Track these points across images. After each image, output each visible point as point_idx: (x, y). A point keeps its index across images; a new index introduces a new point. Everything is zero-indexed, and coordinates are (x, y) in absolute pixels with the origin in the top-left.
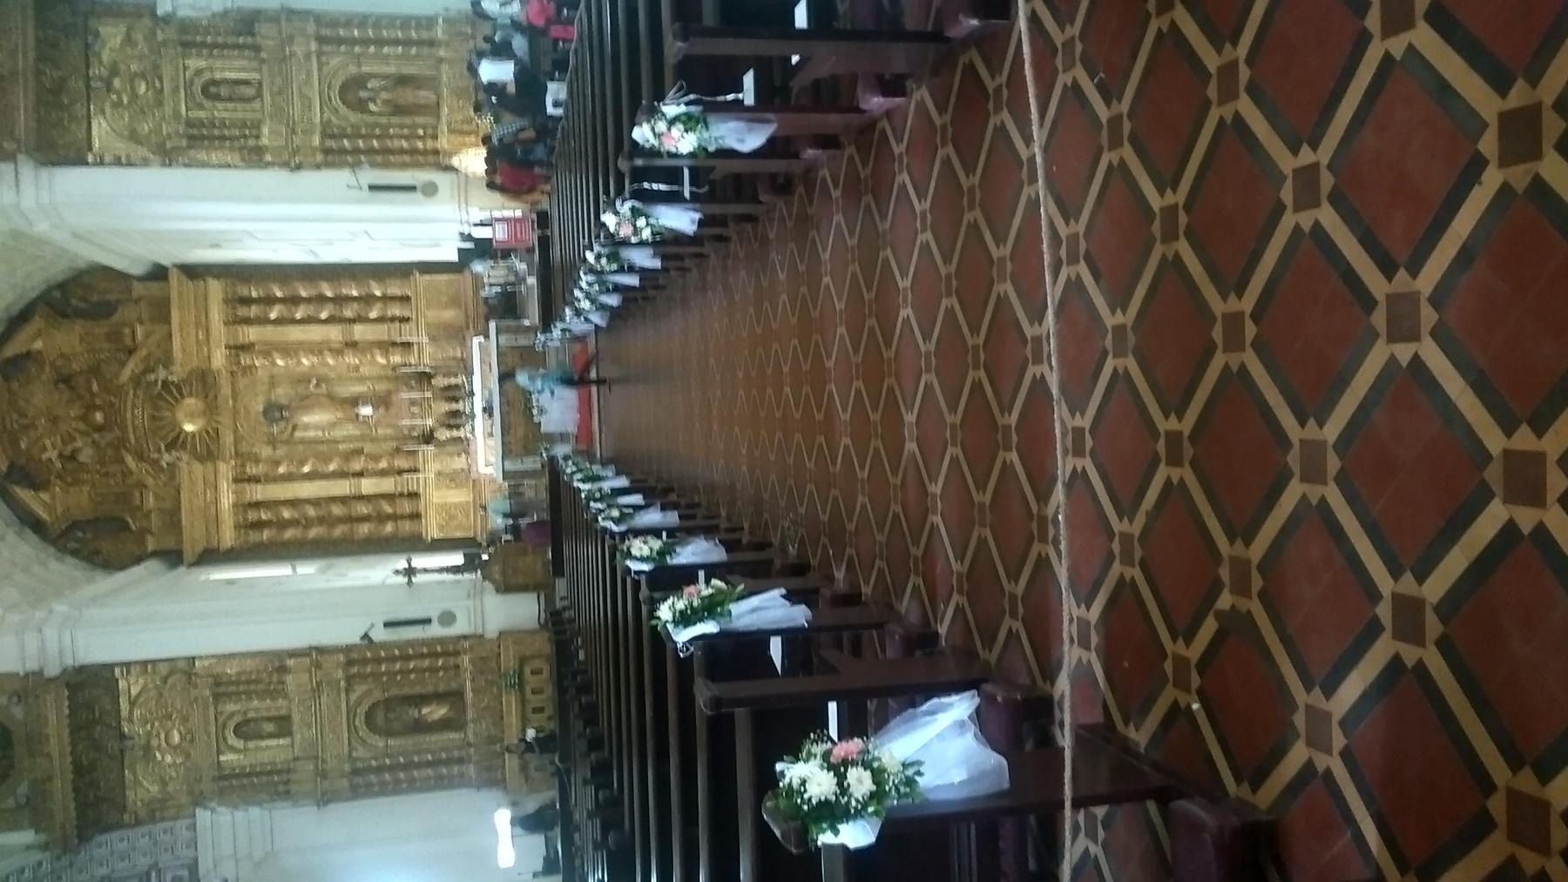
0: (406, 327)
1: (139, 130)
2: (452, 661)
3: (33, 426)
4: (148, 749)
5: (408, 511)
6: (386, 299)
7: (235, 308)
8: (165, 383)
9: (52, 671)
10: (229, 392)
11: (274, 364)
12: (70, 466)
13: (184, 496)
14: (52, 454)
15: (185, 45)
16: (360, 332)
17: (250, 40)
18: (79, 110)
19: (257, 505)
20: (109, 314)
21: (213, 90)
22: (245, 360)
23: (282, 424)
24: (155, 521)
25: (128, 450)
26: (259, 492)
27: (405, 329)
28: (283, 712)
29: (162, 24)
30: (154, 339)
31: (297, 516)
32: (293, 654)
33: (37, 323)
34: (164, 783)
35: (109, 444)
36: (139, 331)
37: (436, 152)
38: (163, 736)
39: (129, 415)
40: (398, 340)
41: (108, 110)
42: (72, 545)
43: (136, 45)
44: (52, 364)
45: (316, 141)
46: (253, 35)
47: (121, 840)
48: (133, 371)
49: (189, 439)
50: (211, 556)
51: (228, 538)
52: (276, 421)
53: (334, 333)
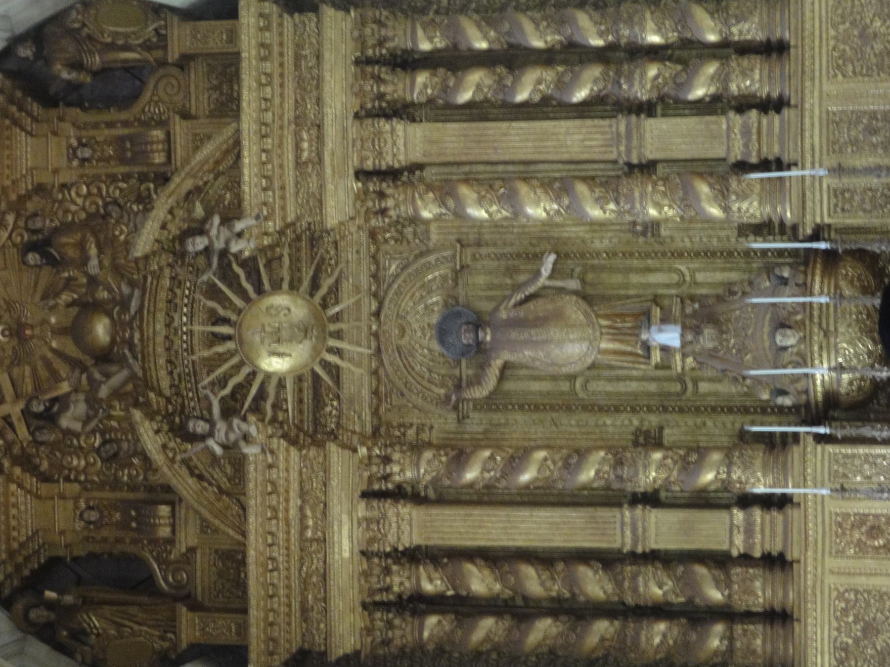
8: (224, 253)
11: (459, 214)
13: (253, 522)
27: (770, 125)
30: (208, 150)
31: (498, 587)
35: (117, 394)
36: (180, 129)
48: (164, 227)
49: (271, 390)
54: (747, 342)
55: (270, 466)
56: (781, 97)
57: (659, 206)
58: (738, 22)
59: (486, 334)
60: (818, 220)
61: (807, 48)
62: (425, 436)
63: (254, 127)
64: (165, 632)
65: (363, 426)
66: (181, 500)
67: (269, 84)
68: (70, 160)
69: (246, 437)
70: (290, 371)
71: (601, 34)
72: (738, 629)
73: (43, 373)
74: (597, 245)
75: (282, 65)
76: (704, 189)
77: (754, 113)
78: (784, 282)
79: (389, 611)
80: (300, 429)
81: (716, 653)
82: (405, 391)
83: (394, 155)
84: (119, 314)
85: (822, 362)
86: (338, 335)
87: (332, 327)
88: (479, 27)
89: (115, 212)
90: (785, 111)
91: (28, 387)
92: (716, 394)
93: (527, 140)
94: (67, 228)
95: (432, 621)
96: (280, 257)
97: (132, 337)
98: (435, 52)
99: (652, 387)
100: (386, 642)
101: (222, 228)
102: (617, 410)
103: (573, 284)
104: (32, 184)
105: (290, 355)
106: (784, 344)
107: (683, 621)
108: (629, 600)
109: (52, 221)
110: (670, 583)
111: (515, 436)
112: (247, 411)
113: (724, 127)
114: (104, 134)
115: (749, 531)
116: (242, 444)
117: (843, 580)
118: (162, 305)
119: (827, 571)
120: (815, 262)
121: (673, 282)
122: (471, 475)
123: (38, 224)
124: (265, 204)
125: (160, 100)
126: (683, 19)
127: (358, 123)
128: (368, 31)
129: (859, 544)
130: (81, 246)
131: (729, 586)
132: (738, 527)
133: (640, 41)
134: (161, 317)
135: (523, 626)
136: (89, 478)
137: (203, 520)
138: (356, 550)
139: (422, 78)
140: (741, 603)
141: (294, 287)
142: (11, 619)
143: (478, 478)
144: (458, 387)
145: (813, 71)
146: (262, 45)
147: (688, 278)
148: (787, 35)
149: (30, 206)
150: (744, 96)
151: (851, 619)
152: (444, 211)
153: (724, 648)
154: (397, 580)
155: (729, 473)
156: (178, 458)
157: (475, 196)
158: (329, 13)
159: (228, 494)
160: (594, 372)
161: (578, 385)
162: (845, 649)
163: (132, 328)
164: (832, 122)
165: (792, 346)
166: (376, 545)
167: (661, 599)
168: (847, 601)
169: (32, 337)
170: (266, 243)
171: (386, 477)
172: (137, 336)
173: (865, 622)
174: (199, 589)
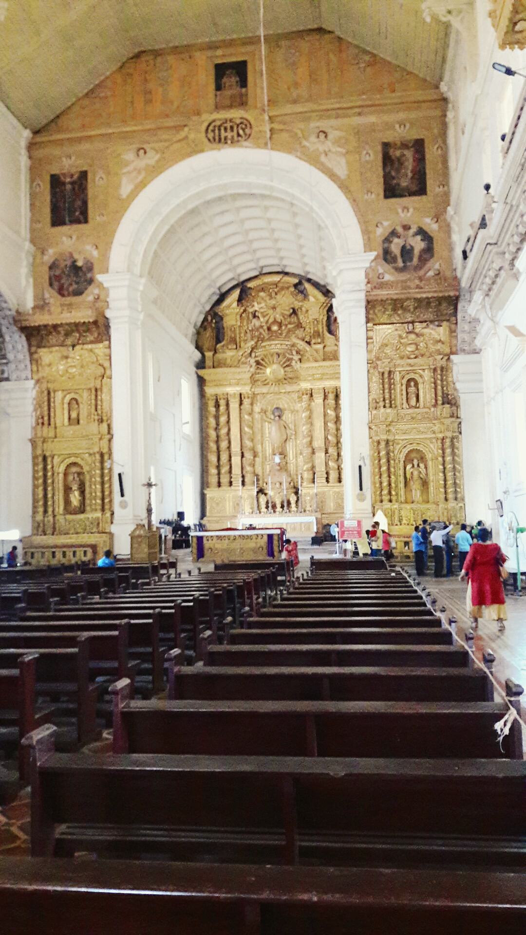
0: (325, 481)
1: (387, 348)
2: (99, 507)
3: (271, 297)
4: (67, 357)
5: (222, 480)
7: (333, 392)
8: (292, 359)
9: (108, 314)
10: (288, 390)
11: (303, 412)
13: (233, 370)
15: (435, 370)
16: (320, 456)
17: (440, 402)
18: (396, 319)
19: (227, 405)
20: (330, 332)
21: (412, 384)
22: (306, 397)
24: (219, 356)
25: (256, 343)
26: (234, 405)
28: (81, 422)
29: (446, 358)
32: (109, 426)
33: (322, 298)
34: (50, 365)
35: (261, 334)
36: (320, 346)
37: (382, 501)
38: (73, 364)
39: (277, 342)
41: (396, 333)
42: (209, 318)
43: (434, 345)
44: (302, 306)
45: (385, 437)
46: (443, 404)
47: (23, 346)
50: (201, 381)
51: (210, 391)
52: (273, 413)
53: (319, 443)
72: (217, 476)
73: (265, 314)
74: (298, 442)
76: (310, 465)
91: (262, 310)
94: (298, 319)
99: (268, 455)
108: (221, 453)
114: (320, 327)
140: (221, 476)
149: (304, 309)
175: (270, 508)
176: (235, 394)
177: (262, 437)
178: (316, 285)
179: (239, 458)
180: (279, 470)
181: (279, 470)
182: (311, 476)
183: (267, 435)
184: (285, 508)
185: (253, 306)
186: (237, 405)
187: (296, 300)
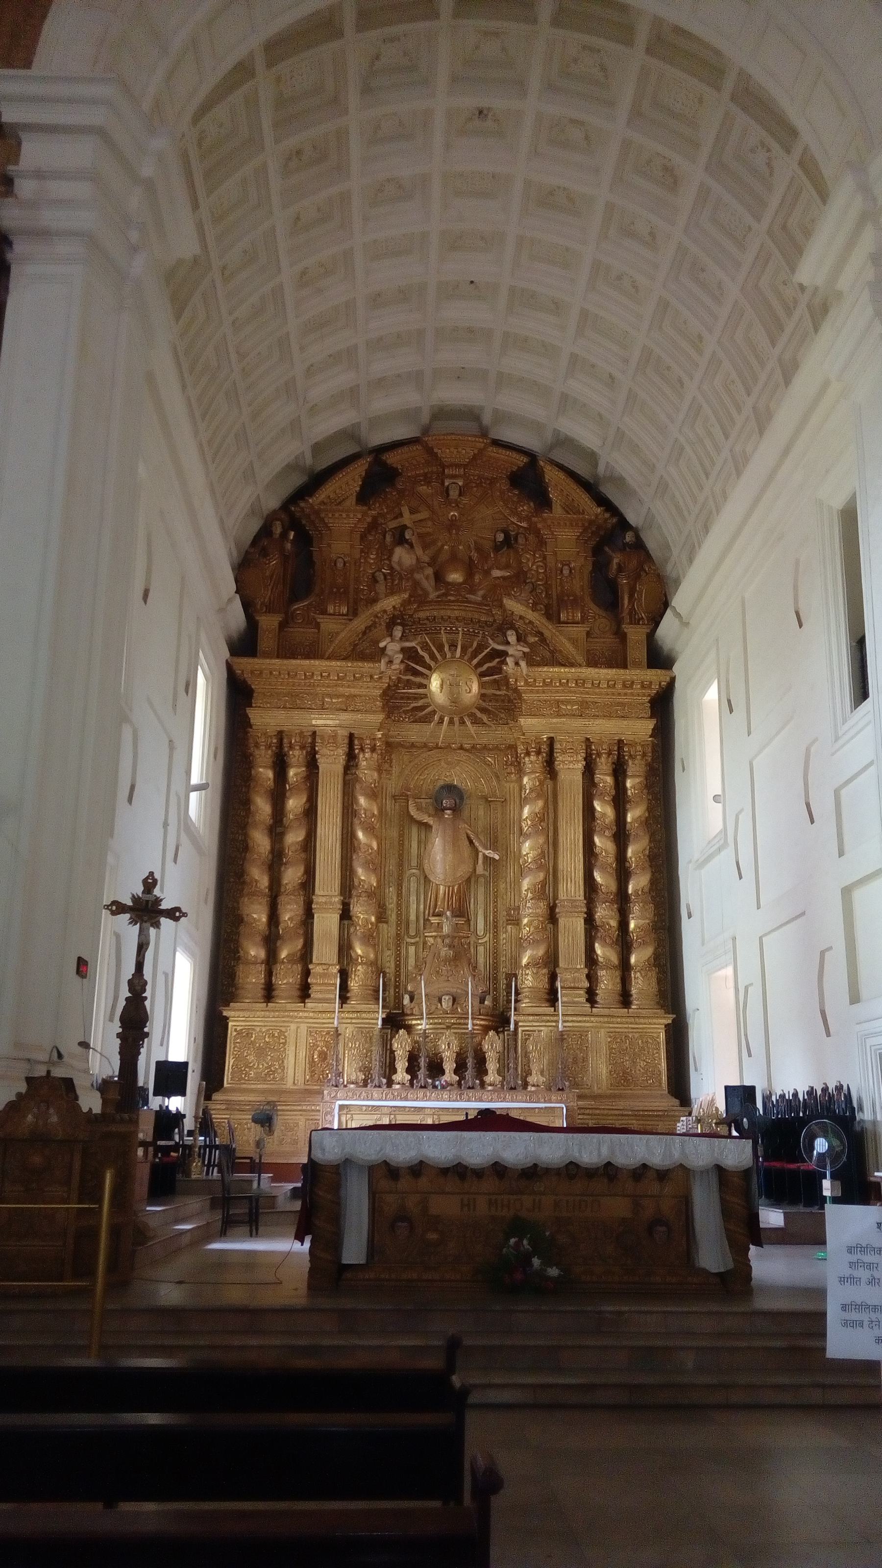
6: (625, 967)
8: (505, 654)
12: (388, 538)
14: (407, 518)
19: (312, 765)
22: (533, 763)
23: (431, 810)
35: (416, 584)
40: (559, 985)
42: (278, 529)
48: (521, 617)
49: (418, 680)
54: (442, 977)
55: (371, 677)
56: (596, 1002)
57: (529, 924)
58: (643, 978)
59: (449, 815)
60: (520, 1024)
61: (628, 1020)
62: (384, 775)
63: (583, 676)
64: (266, 606)
65: (392, 737)
66: (350, 620)
67: (609, 687)
68: (561, 562)
69: (391, 662)
70: (430, 690)
71: (636, 892)
74: (502, 886)
75: (619, 694)
76: (540, 951)
77: (587, 985)
78: (482, 1001)
79: (277, 747)
80: (391, 698)
81: (248, 953)
82: (412, 764)
83: (563, 762)
84: (463, 588)
85: (431, 1024)
86: (451, 722)
87: (456, 719)
88: (640, 817)
89: (528, 588)
90: (589, 1005)
92: (407, 957)
93: (571, 844)
95: (270, 774)
96: (499, 689)
97: (451, 595)
98: (625, 789)
99: (413, 917)
100: (257, 745)
101: (522, 653)
102: (399, 895)
103: (480, 869)
104: (547, 538)
105: (441, 692)
106: (443, 1000)
107: (267, 933)
108: (282, 899)
109: (522, 549)
110: (292, 925)
111: (384, 831)
112: (407, 663)
113: (579, 967)
115: (324, 975)
116: (387, 659)
117: (293, 1035)
118: (470, 615)
119: (298, 1025)
120: (493, 1021)
121: (478, 933)
122: (362, 800)
123: (521, 540)
124: (535, 681)
125: (596, 620)
126: (644, 943)
127: (583, 739)
128: (639, 748)
129: (315, 1046)
130: (507, 567)
131: (289, 962)
132: (327, 969)
133: (631, 916)
134: (463, 614)
135: (266, 831)
136: (362, 565)
137: (338, 633)
138: (316, 729)
139: (609, 780)
141: (483, 696)
142: (274, 512)
143: (361, 806)
144: (416, 797)
145: (612, 1023)
146: (633, 683)
147: (480, 941)
148: (635, 1007)
150: (597, 979)
151: (267, 1040)
152: (527, 791)
153: (250, 958)
154: (297, 753)
155: (362, 963)
156: (377, 620)
157: (537, 811)
158: (650, 724)
159: (353, 649)
160: (422, 881)
161: (414, 871)
162: (249, 1035)
163: (456, 595)
164: (582, 1034)
165: (441, 1005)
166: (320, 741)
167: (281, 919)
168: (279, 1038)
169: (451, 534)
170: (510, 680)
171: (362, 750)
172: (452, 598)
173: (265, 1049)
174: (292, 630)
175: (422, 1074)
176: (335, 736)
177: (400, 865)
178: (572, 475)
179: (335, 917)
180: (447, 961)
181: (447, 961)
182: (544, 984)
183: (414, 863)
184: (469, 1073)
185: (401, 515)
186: (339, 768)
187: (514, 512)
